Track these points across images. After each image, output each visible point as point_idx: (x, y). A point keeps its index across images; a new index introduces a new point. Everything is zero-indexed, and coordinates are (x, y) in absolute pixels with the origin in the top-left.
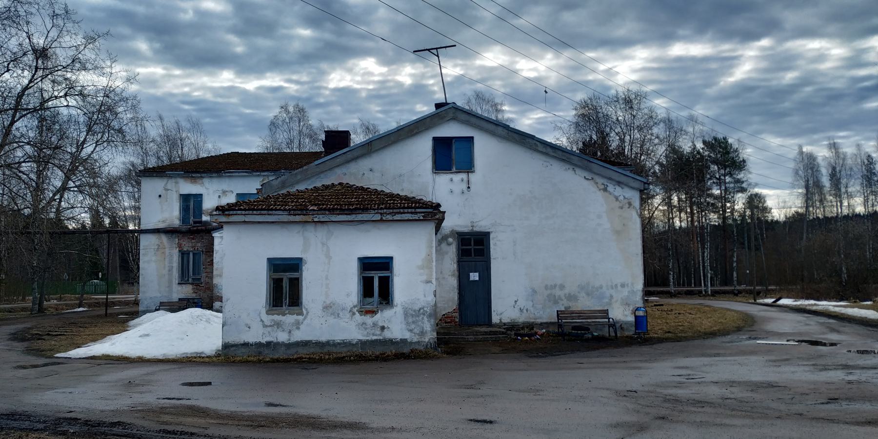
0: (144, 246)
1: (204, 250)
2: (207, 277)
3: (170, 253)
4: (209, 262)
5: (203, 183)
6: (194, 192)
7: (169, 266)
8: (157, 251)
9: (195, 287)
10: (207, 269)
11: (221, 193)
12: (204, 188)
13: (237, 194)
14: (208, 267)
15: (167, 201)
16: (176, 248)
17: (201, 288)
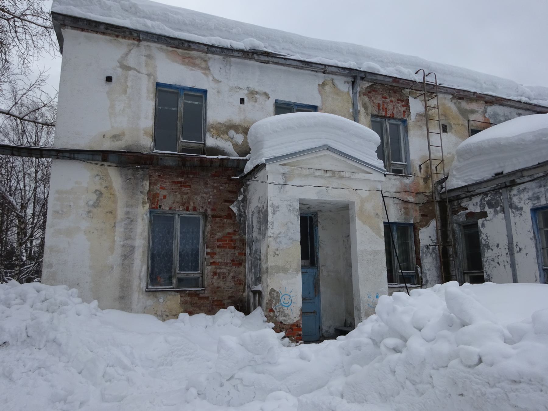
0: (57, 192)
1: (209, 211)
2: (215, 274)
3: (127, 213)
4: (218, 240)
5: (207, 69)
6: (189, 84)
7: (123, 246)
8: (94, 206)
9: (188, 298)
10: (216, 257)
11: (246, 94)
12: (211, 78)
13: (276, 100)
14: (218, 250)
15: (126, 92)
16: (144, 203)
17: (202, 302)
